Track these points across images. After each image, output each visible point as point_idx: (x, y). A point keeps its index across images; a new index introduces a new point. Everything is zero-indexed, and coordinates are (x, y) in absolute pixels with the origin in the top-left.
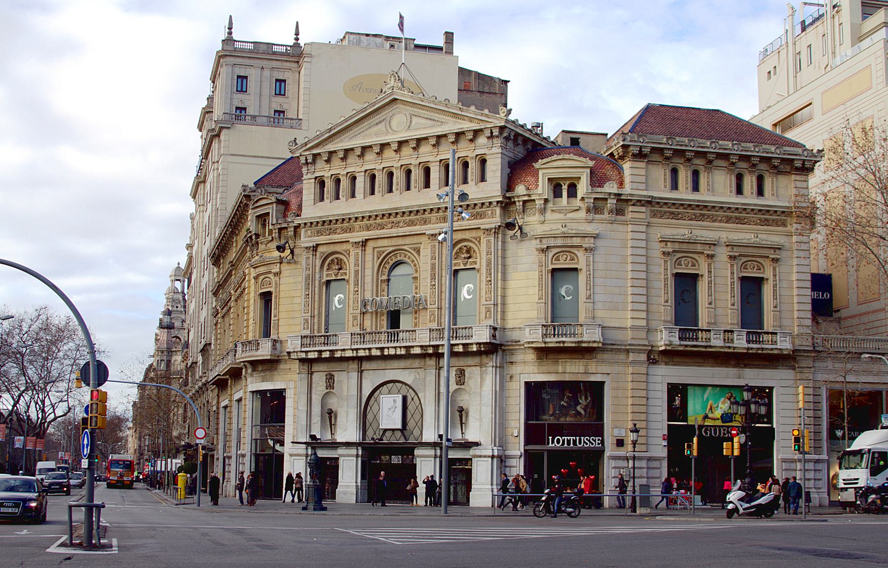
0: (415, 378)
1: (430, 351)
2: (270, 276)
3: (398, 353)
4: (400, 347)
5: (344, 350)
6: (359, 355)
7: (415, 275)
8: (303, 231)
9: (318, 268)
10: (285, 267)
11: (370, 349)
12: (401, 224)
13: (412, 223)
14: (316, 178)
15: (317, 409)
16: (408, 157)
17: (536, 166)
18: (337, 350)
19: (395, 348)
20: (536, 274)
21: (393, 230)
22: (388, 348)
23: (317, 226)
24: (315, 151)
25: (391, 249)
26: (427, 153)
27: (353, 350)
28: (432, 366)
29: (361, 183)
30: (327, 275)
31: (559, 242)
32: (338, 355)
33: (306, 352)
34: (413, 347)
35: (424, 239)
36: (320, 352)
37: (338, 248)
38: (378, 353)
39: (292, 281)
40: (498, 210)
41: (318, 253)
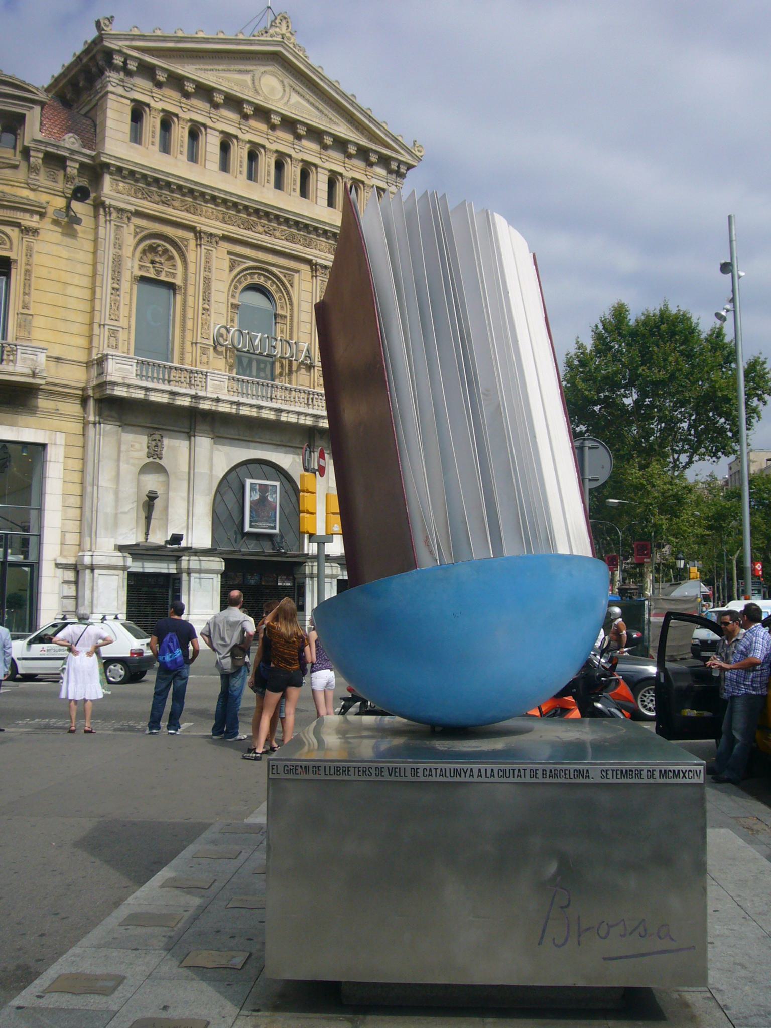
0: (294, 461)
2: (7, 229)
3: (302, 421)
4: (306, 415)
5: (218, 400)
6: (242, 412)
7: (280, 312)
8: (107, 179)
9: (131, 249)
10: (46, 226)
11: (260, 407)
12: (277, 234)
13: (291, 239)
14: (133, 100)
16: (282, 141)
18: (205, 398)
19: (299, 413)
21: (264, 237)
22: (288, 412)
23: (137, 181)
24: (148, 59)
25: (252, 263)
26: (309, 150)
27: (232, 403)
29: (211, 144)
30: (141, 267)
32: (205, 405)
33: (147, 389)
35: (305, 268)
36: (173, 393)
38: (272, 416)
39: (65, 253)
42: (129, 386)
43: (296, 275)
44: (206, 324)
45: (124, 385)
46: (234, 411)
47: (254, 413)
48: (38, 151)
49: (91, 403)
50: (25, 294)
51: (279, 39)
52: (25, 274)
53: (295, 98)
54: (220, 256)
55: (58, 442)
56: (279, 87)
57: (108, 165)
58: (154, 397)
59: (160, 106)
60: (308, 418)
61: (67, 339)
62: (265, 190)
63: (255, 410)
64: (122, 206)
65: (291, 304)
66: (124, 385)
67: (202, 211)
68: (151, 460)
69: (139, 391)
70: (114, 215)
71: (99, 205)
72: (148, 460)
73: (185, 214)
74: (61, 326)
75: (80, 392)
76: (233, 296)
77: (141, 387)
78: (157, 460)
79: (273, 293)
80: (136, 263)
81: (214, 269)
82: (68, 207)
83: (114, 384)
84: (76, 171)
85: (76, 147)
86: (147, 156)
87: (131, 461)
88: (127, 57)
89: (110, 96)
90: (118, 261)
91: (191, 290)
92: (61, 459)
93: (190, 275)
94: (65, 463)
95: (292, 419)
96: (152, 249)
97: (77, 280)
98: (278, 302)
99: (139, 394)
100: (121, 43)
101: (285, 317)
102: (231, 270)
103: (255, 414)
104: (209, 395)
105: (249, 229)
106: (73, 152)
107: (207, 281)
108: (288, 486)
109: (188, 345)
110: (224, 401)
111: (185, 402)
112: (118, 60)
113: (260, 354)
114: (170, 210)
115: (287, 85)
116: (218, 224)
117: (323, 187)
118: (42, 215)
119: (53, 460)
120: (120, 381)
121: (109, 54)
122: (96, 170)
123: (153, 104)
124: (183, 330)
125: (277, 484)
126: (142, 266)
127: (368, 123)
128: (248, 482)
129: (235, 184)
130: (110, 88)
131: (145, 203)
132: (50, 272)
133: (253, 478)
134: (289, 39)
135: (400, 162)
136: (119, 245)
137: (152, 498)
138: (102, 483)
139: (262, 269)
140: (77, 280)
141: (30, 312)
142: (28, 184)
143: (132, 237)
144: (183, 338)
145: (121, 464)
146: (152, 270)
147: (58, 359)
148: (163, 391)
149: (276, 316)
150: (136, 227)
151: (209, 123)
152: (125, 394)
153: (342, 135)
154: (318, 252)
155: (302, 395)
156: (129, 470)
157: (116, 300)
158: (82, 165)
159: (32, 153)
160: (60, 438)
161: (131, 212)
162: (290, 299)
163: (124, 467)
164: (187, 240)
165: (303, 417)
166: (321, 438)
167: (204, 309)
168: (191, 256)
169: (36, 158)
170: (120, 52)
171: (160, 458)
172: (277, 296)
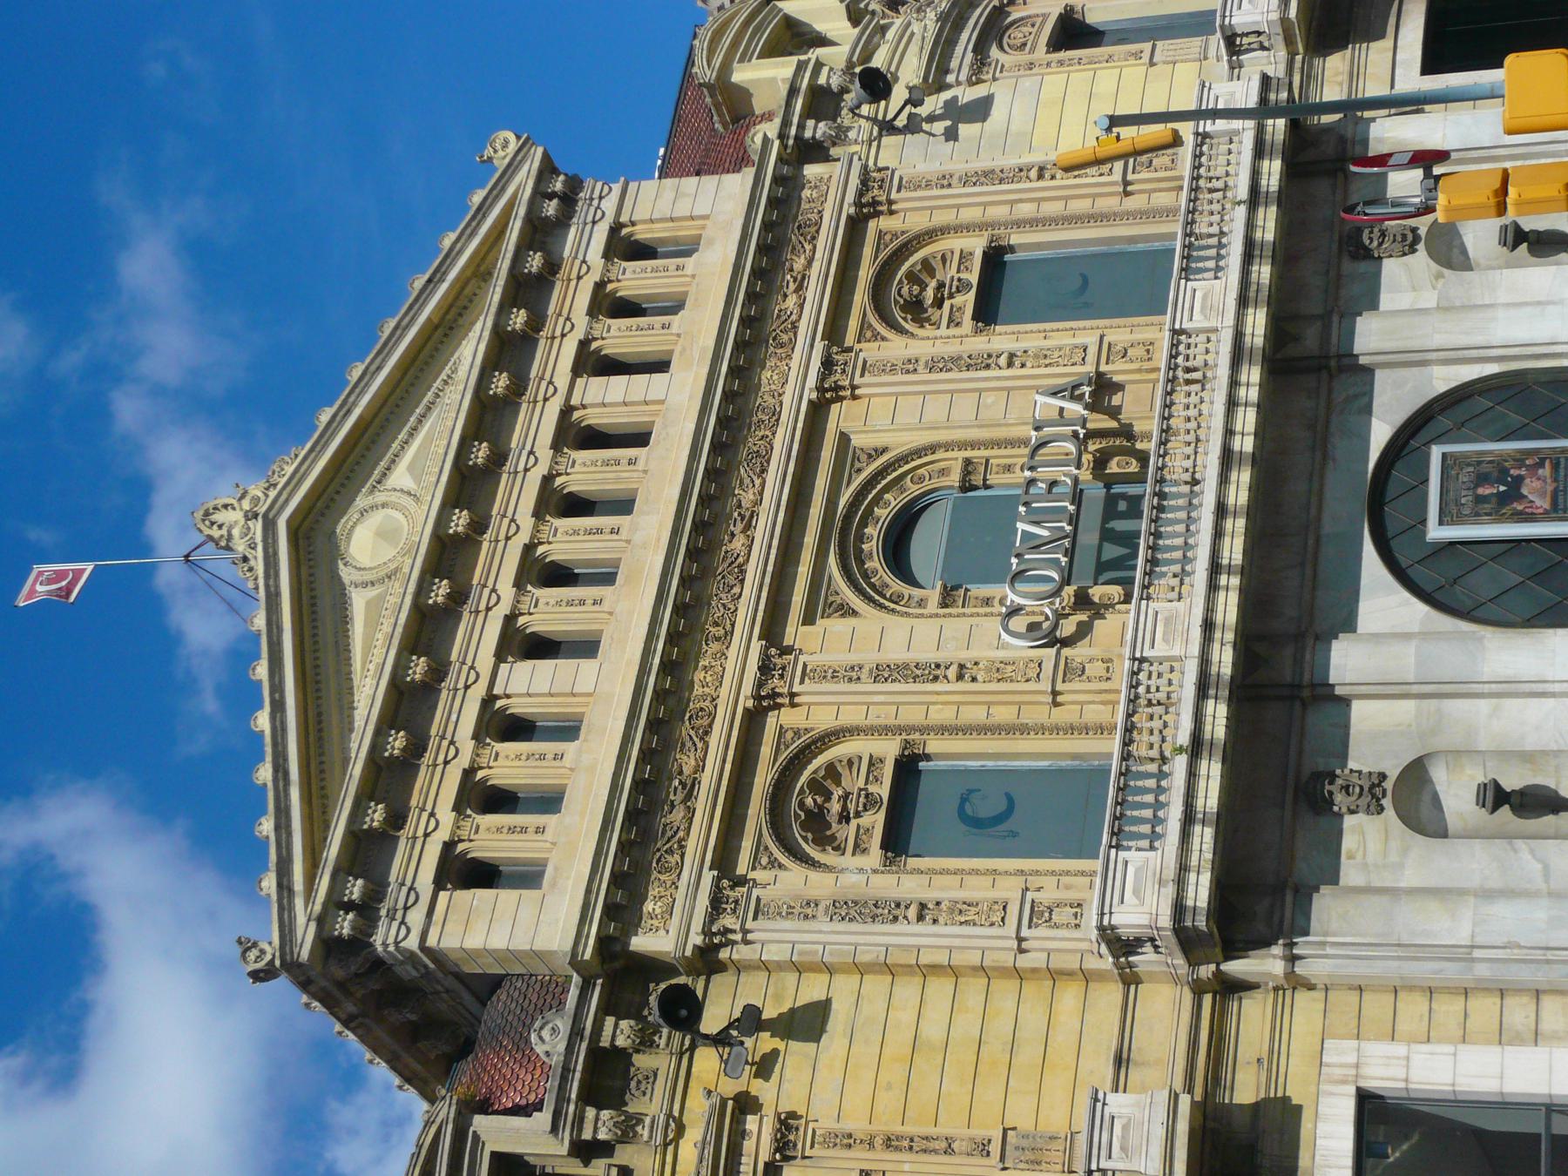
1: (1263, 272)
3: (1254, 394)
4: (1234, 383)
5: (1208, 626)
7: (955, 478)
8: (641, 943)
9: (814, 876)
11: (1221, 511)
15: (1470, 862)
17: (704, 71)
18: (1205, 661)
19: (1232, 404)
20: (1054, 82)
22: (1229, 432)
25: (832, 560)
27: (1213, 587)
28: (1327, 328)
31: (968, 36)
32: (1224, 660)
33: (1189, 819)
34: (1239, 336)
37: (763, 778)
38: (1242, 478)
40: (811, 171)
41: (758, 875)
42: (1183, 868)
43: (857, 441)
44: (999, 672)
45: (1180, 882)
46: (1235, 581)
47: (1237, 527)
48: (579, 1120)
49: (1235, 967)
50: (949, 1150)
51: (257, 527)
52: (897, 1149)
53: (400, 477)
54: (819, 642)
55: (1352, 1059)
56: (376, 518)
57: (603, 942)
58: (1210, 796)
59: (446, 816)
60: (1243, 378)
61: (1063, 1038)
62: (637, 538)
63: (1229, 524)
64: (703, 901)
65: (933, 448)
66: (1180, 882)
67: (704, 697)
68: (1387, 802)
69: (1196, 841)
70: (728, 921)
71: (708, 960)
72: (1390, 812)
73: (715, 740)
74: (1028, 1054)
75: (1207, 999)
76: (921, 603)
77: (1185, 835)
78: (1389, 785)
79: (904, 498)
80: (848, 860)
81: (854, 658)
82: (720, 1040)
83: (1179, 909)
84: (624, 1024)
85: (563, 1024)
86: (571, 845)
87: (1394, 857)
88: (336, 903)
89: (432, 941)
90: (848, 909)
91: (912, 715)
92: (1400, 1049)
93: (872, 720)
94: (1412, 1040)
95: (1247, 419)
96: (817, 823)
97: (904, 1016)
98: (928, 485)
99: (1204, 838)
100: (301, 919)
101: (968, 462)
102: (855, 613)
103: (1241, 523)
104: (1195, 650)
105: (743, 572)
106: (576, 1033)
107: (883, 673)
108: (1443, 422)
109: (1060, 716)
110: (1210, 609)
111: (1218, 715)
112: (345, 925)
113: (1074, 520)
114: (707, 779)
115: (370, 501)
116: (732, 652)
117: (617, 387)
118: (746, 1104)
119: (1401, 1074)
120: (1169, 891)
121: (328, 945)
122: (619, 973)
123: (443, 835)
124: (1023, 730)
125: (1436, 452)
126: (856, 846)
127: (444, 287)
128: (1437, 532)
129: (627, 617)
130: (412, 943)
131: (692, 845)
132: (889, 1086)
133: (1424, 522)
134: (256, 500)
135: (540, 194)
136: (806, 909)
137: (1496, 797)
138: (1462, 935)
139: (844, 534)
140: (904, 1016)
141: (997, 1135)
142: (666, 1145)
143: (782, 874)
144: (1041, 729)
145: (1402, 885)
146: (866, 820)
147: (1121, 1061)
148: (1192, 774)
149: (967, 486)
150: (755, 864)
151: (479, 691)
152: (1206, 878)
153: (482, 347)
154: (789, 388)
155: (1180, 398)
156: (1421, 862)
157: (951, 910)
158: (606, 1008)
159: (587, 1135)
160: (1341, 1053)
161: (719, 879)
162: (918, 452)
163: (1410, 878)
164: (782, 731)
165: (1242, 392)
166: (1296, 339)
167: (960, 677)
168: (822, 719)
169: (600, 1124)
170: (321, 921)
171: (1383, 776)
172: (913, 490)
